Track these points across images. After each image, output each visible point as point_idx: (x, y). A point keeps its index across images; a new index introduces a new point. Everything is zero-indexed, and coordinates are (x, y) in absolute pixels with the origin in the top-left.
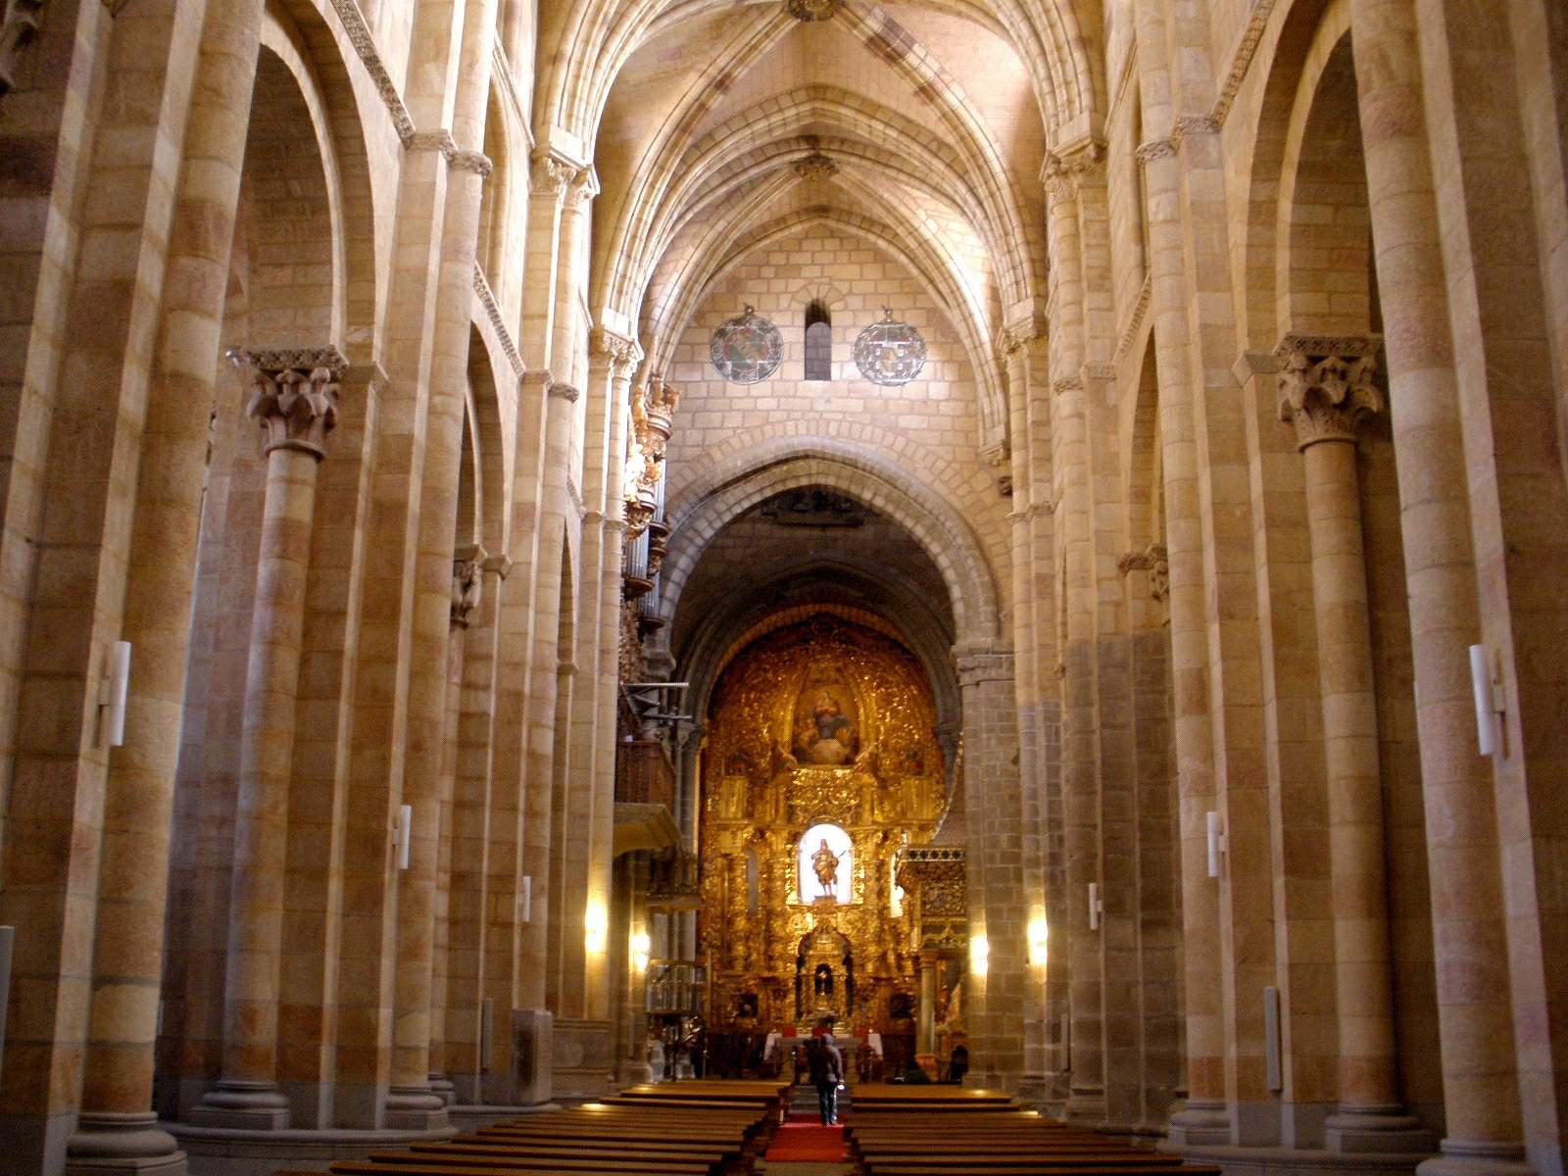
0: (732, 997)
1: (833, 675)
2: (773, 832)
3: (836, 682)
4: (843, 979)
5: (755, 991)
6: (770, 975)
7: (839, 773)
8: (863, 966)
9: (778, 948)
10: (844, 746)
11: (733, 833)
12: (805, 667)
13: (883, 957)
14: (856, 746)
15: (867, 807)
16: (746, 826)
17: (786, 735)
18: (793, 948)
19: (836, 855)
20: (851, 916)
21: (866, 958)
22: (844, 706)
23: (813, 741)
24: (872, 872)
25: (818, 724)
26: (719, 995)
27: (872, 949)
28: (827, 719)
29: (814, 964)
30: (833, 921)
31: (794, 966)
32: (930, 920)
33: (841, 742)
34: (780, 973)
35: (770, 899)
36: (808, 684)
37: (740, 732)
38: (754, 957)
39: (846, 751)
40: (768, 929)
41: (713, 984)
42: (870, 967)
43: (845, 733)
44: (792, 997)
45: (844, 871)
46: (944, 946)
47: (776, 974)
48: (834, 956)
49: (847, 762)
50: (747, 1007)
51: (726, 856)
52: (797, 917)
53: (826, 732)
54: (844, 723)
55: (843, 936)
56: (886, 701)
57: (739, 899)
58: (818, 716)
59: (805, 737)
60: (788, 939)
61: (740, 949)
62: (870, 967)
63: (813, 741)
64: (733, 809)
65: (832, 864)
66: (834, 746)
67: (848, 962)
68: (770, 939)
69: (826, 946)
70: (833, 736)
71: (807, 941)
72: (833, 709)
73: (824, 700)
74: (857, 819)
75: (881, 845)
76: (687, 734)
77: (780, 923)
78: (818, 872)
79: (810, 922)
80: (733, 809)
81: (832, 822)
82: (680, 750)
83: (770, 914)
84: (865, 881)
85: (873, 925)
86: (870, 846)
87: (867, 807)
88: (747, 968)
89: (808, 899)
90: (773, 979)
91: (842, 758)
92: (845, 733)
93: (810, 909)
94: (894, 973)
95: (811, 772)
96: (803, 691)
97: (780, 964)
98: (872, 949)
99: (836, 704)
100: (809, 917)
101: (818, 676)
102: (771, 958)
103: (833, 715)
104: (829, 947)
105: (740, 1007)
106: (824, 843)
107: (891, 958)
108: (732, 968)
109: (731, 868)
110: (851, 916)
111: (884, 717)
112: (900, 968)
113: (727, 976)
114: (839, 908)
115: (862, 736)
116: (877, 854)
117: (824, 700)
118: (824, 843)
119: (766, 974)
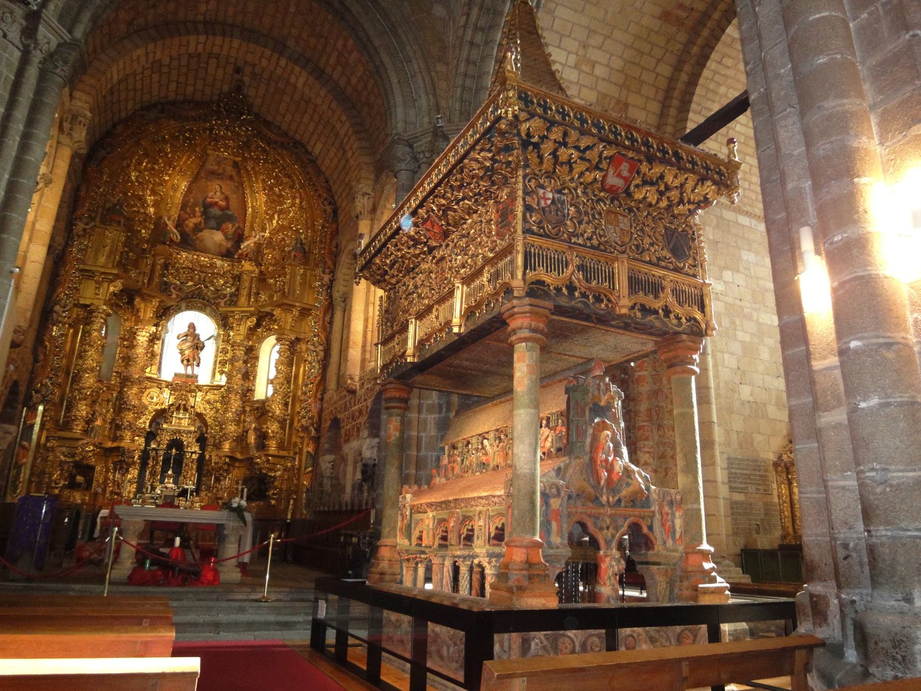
0: (62, 463)
1: (229, 169)
2: (143, 299)
3: (231, 178)
4: (194, 456)
5: (92, 461)
6: (115, 445)
7: (219, 263)
8: (218, 446)
9: (130, 416)
10: (227, 239)
11: (97, 282)
12: (204, 151)
13: (241, 439)
14: (239, 238)
15: (245, 292)
16: (117, 277)
17: (175, 213)
18: (144, 422)
19: (202, 339)
20: (210, 396)
21: (225, 437)
22: (234, 203)
23: (197, 229)
24: (240, 353)
25: (205, 213)
26: (45, 460)
27: (232, 428)
28: (215, 211)
29: (165, 439)
30: (192, 401)
31: (142, 440)
32: (538, 241)
33: (225, 234)
34: (126, 443)
35: (127, 365)
36: (203, 174)
37: (125, 194)
38: (99, 422)
39: (229, 245)
40: (121, 396)
41: (38, 444)
42: (227, 446)
43: (230, 227)
44: (134, 473)
45: (208, 355)
46: (563, 302)
47: (122, 444)
48: (190, 432)
49: (227, 255)
50: (79, 479)
51: (86, 306)
52: (154, 391)
53: (213, 223)
54: (230, 218)
55: (200, 416)
56: (275, 201)
57: (92, 353)
58: (207, 206)
59: (191, 222)
60: (140, 411)
61: (83, 410)
62: (227, 446)
63: (197, 229)
64: (102, 260)
65: (198, 346)
66: (218, 237)
67: (202, 440)
68: (121, 406)
69: (182, 422)
70: (218, 228)
71: (162, 415)
72: (223, 203)
73: (216, 192)
74: (233, 300)
75: (252, 330)
76: (54, 42)
77: (135, 390)
78: (182, 352)
79: (166, 398)
80: (102, 260)
81: (201, 309)
82: (37, 57)
83: (125, 381)
84: (232, 361)
85: (235, 403)
86: (243, 329)
87: (245, 292)
88: (86, 432)
89: (167, 375)
90: (118, 448)
91: (224, 250)
92: (230, 227)
93: (169, 385)
94: (254, 453)
95: (190, 256)
96: (196, 179)
97: (128, 435)
98: (232, 428)
99: (227, 199)
100: (167, 392)
101: (216, 167)
102: (118, 427)
103: (222, 209)
104: (185, 422)
105: (72, 477)
106: (192, 326)
107: (252, 438)
108: (70, 430)
109: (88, 321)
110: (210, 396)
111: (272, 218)
112: (262, 446)
113: (61, 438)
114: (199, 388)
115: (246, 233)
116: (248, 337)
117: (216, 192)
118: (192, 326)
119: (109, 444)
